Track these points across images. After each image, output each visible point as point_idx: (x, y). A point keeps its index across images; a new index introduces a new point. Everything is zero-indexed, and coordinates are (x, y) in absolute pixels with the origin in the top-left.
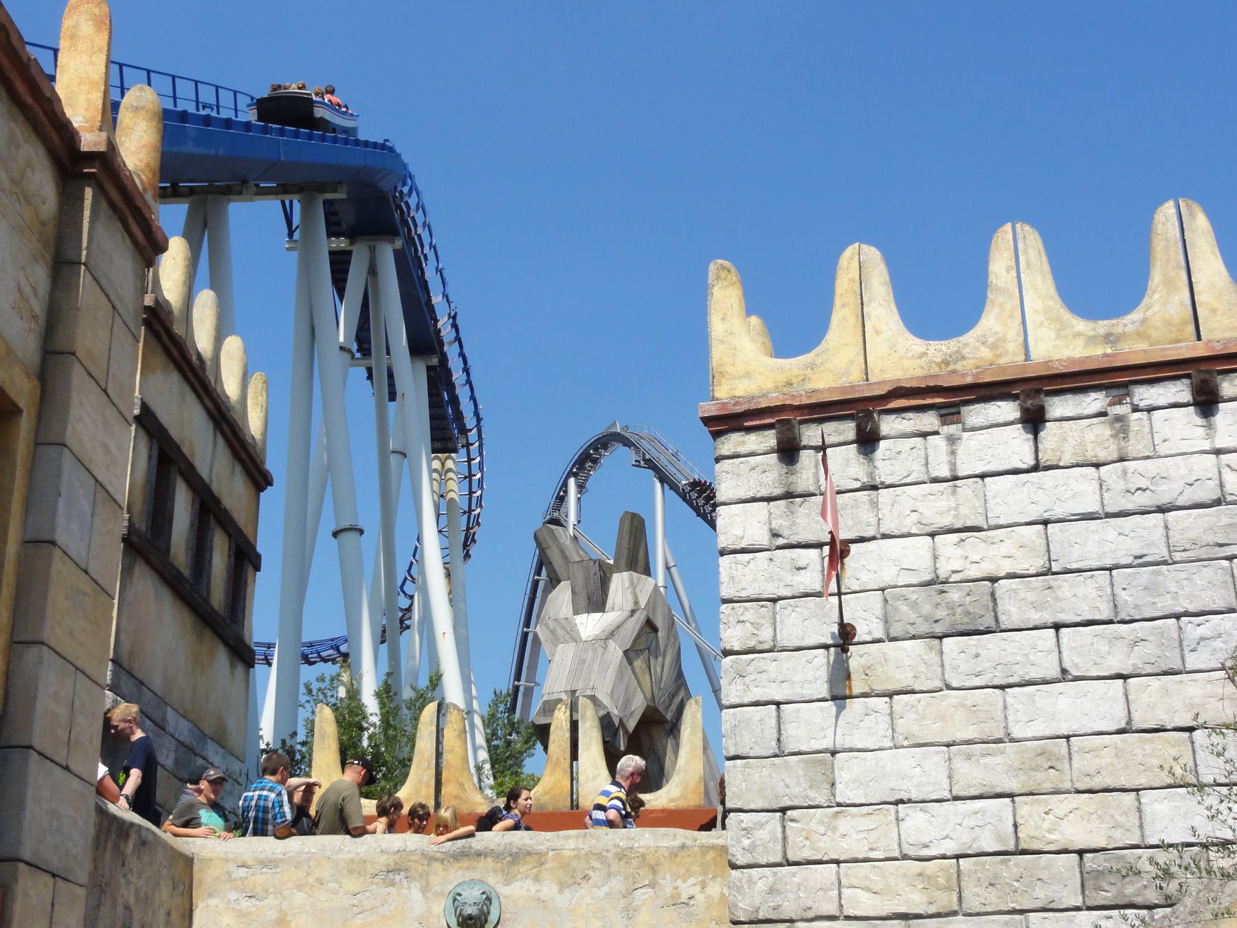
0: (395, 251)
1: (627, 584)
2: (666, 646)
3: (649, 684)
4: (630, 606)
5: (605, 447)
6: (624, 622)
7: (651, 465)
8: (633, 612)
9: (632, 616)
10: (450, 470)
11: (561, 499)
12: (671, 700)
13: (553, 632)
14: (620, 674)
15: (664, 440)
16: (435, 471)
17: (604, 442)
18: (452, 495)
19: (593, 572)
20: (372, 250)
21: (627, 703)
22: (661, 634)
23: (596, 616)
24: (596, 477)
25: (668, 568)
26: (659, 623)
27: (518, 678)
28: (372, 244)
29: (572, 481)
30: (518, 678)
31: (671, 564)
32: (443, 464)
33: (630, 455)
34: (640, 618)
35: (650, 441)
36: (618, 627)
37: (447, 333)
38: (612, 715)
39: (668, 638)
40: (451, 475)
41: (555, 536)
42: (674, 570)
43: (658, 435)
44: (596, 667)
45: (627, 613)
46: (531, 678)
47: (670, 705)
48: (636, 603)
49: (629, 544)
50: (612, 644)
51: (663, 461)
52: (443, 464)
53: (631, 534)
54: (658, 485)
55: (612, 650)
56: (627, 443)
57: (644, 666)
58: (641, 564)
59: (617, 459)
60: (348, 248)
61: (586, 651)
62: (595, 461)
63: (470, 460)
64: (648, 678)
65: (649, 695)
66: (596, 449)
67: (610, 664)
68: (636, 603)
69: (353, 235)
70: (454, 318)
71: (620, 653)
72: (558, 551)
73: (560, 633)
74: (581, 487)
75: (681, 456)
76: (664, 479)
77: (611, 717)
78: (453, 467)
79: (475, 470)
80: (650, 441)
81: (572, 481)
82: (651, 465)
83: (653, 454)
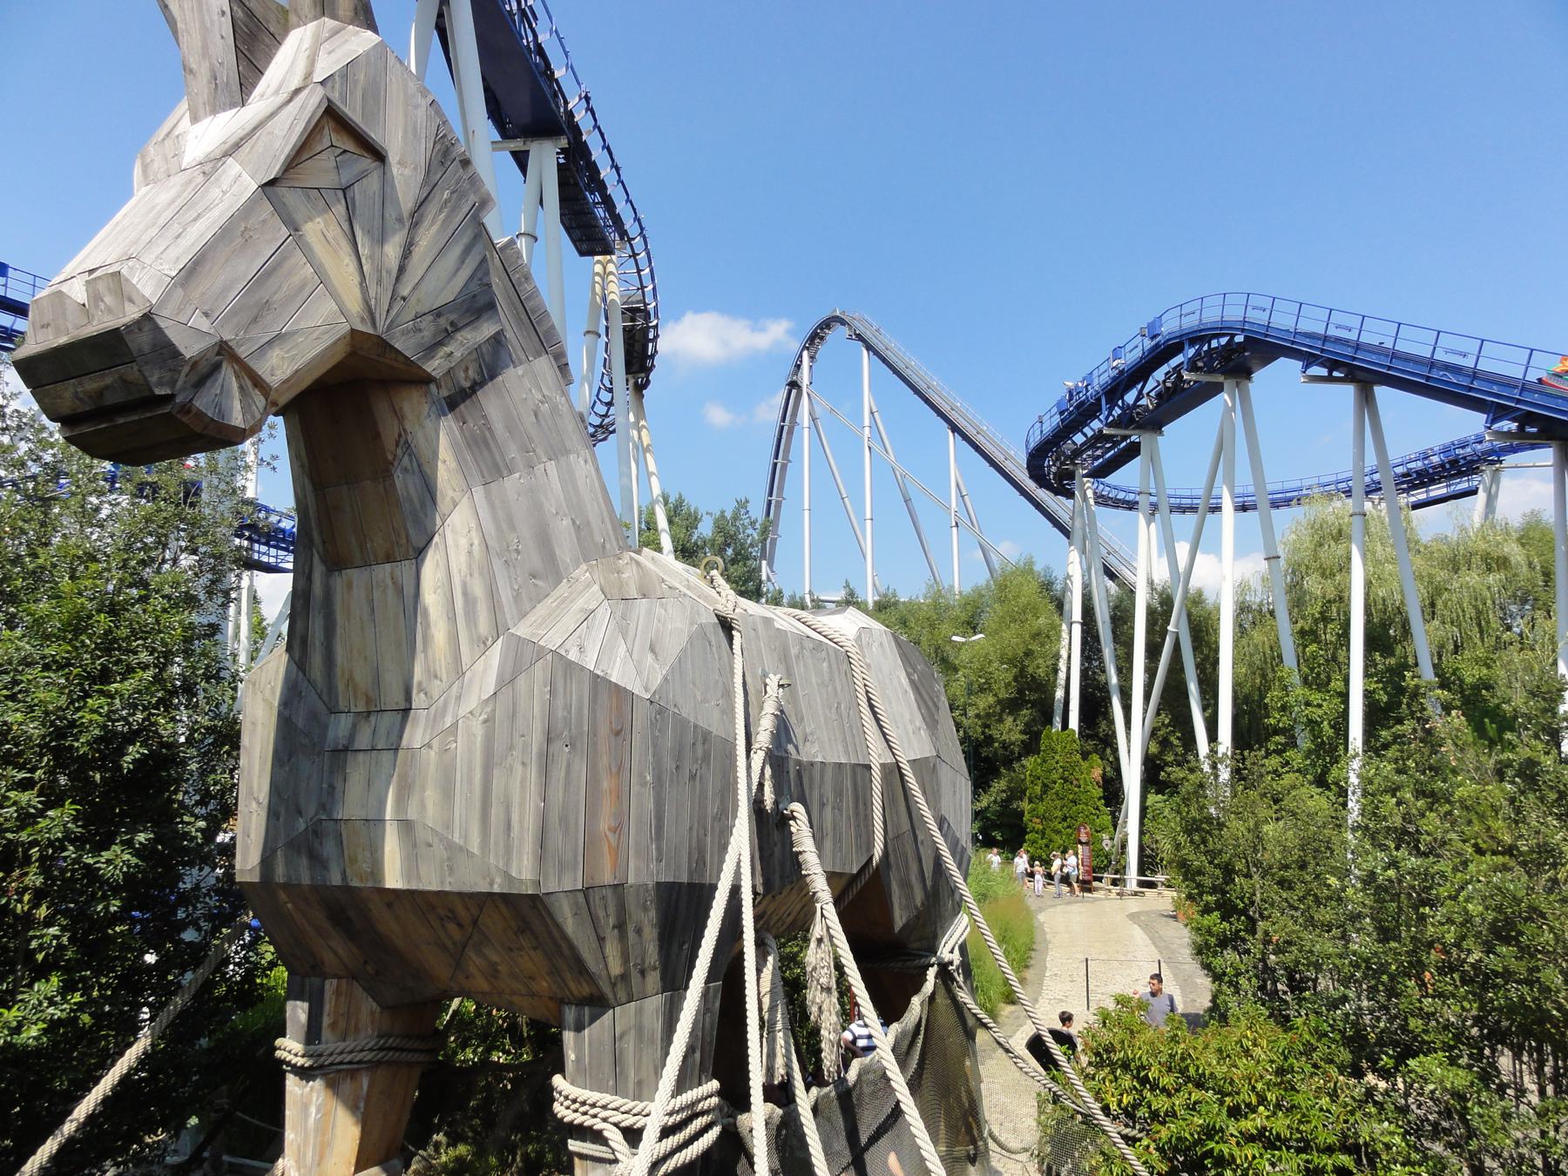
2: (421, 204)
4: (295, 83)
5: (828, 327)
7: (860, 337)
10: (611, 273)
11: (798, 367)
12: (446, 336)
14: (232, 233)
16: (598, 274)
17: (827, 324)
18: (612, 296)
19: (216, 10)
21: (256, 307)
24: (823, 349)
25: (872, 413)
27: (771, 494)
29: (805, 353)
30: (771, 494)
32: (605, 268)
33: (845, 331)
34: (310, 103)
35: (859, 321)
36: (255, 129)
37: (581, 116)
38: (162, 324)
40: (611, 278)
46: (780, 494)
47: (440, 344)
51: (868, 335)
52: (605, 268)
54: (865, 352)
55: (226, 182)
56: (843, 322)
59: (838, 334)
62: (822, 338)
63: (639, 271)
65: (354, 305)
66: (822, 329)
67: (208, 209)
68: (308, 75)
70: (587, 99)
74: (812, 358)
76: (869, 348)
77: (158, 329)
78: (614, 270)
79: (647, 281)
80: (859, 321)
81: (805, 353)
82: (860, 337)
83: (861, 330)
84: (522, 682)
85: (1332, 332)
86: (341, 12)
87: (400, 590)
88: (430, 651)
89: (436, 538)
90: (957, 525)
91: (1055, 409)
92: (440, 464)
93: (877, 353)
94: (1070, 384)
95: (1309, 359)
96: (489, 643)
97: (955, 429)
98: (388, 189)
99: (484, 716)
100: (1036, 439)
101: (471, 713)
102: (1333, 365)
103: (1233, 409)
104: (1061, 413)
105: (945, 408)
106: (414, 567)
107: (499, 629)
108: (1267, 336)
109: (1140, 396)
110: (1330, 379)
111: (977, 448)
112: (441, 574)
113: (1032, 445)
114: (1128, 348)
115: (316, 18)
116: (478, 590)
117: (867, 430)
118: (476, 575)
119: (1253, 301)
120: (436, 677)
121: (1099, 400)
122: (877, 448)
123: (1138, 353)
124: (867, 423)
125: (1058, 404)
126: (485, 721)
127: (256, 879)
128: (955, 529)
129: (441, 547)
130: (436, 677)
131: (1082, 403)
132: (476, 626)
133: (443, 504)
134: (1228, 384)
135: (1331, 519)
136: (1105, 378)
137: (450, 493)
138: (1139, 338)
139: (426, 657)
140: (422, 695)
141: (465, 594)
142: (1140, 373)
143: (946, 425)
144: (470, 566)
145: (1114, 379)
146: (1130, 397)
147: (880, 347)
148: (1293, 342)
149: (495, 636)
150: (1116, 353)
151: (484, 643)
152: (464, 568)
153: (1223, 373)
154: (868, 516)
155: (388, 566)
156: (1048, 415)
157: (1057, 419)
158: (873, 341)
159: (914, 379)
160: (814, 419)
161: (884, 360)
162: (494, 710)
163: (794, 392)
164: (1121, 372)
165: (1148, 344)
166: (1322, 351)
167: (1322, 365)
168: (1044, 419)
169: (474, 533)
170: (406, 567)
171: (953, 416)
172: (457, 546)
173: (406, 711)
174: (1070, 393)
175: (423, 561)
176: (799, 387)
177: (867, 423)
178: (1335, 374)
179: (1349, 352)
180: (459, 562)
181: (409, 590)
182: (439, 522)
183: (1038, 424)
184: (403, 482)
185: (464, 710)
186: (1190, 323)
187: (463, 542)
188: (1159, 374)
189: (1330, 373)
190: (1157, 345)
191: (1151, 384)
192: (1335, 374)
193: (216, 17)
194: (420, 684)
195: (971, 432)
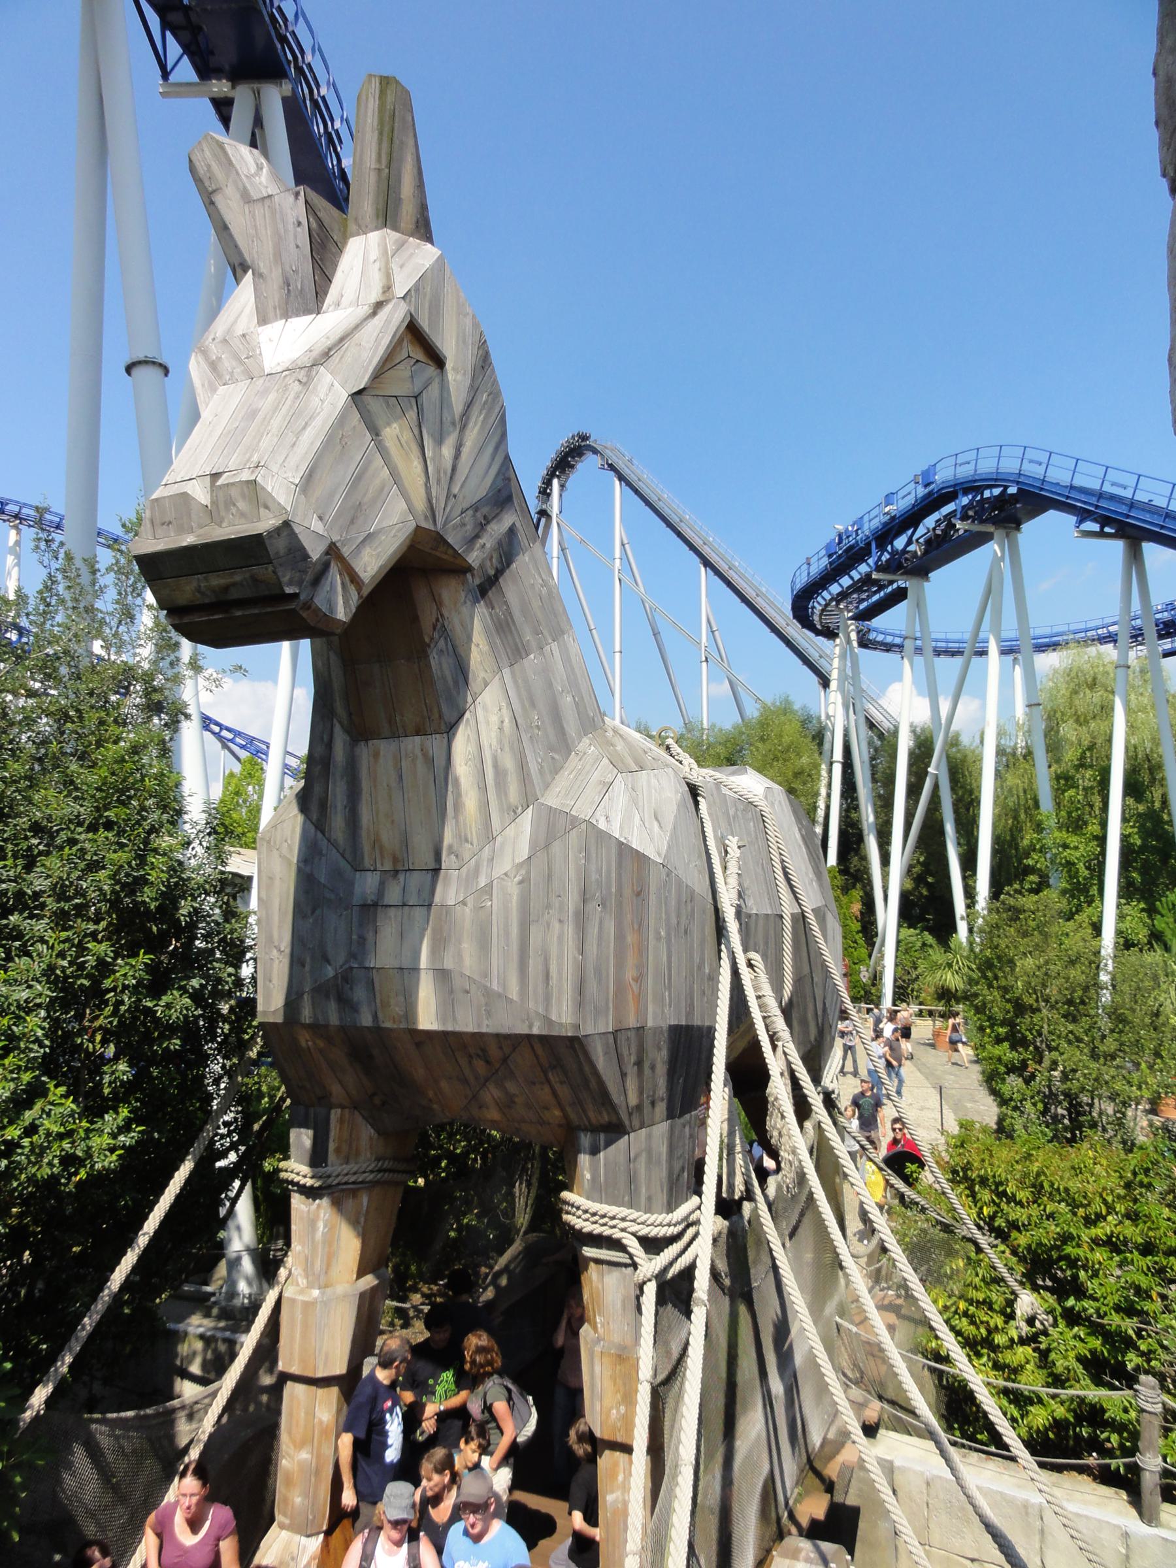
0: (285, 100)
1: (374, 253)
2: (469, 406)
3: (421, 480)
4: (375, 295)
6: (357, 327)
7: (612, 467)
8: (379, 305)
9: (374, 313)
12: (481, 527)
13: (214, 366)
14: (335, 441)
15: (622, 450)
19: (291, 220)
20: (257, 95)
21: (355, 512)
22: (457, 376)
23: (300, 322)
25: (623, 545)
26: (448, 345)
28: (255, 86)
31: (625, 541)
34: (393, 317)
36: (342, 339)
38: (297, 529)
39: (474, 390)
41: (230, 163)
42: (627, 546)
43: (618, 446)
44: (276, 423)
45: (366, 310)
47: (477, 536)
48: (388, 288)
49: (379, 160)
50: (325, 376)
51: (620, 465)
53: (381, 134)
54: (617, 482)
55: (322, 390)
57: (407, 436)
58: (408, 211)
59: (587, 466)
60: (230, 95)
61: (265, 392)
64: (417, 465)
65: (420, 505)
67: (312, 418)
68: (388, 288)
69: (237, 76)
71: (342, 396)
72: (238, 196)
73: (227, 363)
74: (562, 486)
75: (635, 462)
76: (621, 478)
77: (293, 535)
80: (612, 450)
81: (555, 482)
82: (612, 467)
84: (556, 847)
85: (1107, 488)
86: (403, 225)
87: (429, 761)
88: (461, 818)
89: (467, 715)
90: (707, 660)
91: (823, 552)
92: (473, 647)
93: (629, 484)
94: (840, 527)
95: (1083, 515)
96: (519, 811)
97: (707, 563)
98: (445, 395)
99: (518, 878)
100: (802, 580)
101: (506, 874)
102: (1105, 521)
103: (1002, 558)
104: (830, 556)
105: (697, 542)
106: (445, 740)
107: (529, 798)
108: (1042, 489)
109: (909, 542)
110: (1101, 534)
111: (729, 584)
112: (472, 748)
113: (798, 586)
114: (901, 494)
115: (377, 228)
116: (509, 763)
117: (618, 562)
118: (507, 749)
119: (1030, 454)
120: (467, 841)
121: (869, 545)
122: (627, 579)
123: (911, 500)
124: (617, 554)
125: (827, 547)
126: (521, 882)
127: (279, 1019)
128: (704, 664)
129: (473, 723)
130: (467, 841)
131: (851, 547)
132: (506, 795)
133: (475, 683)
134: (998, 534)
135: (1086, 667)
136: (876, 523)
137: (482, 674)
138: (912, 485)
139: (457, 822)
140: (453, 857)
141: (496, 766)
142: (912, 519)
143: (698, 560)
144: (500, 742)
145: (885, 524)
146: (900, 543)
147: (632, 478)
148: (1068, 497)
149: (525, 805)
150: (889, 499)
151: (515, 812)
152: (494, 743)
153: (994, 524)
154: (617, 648)
155: (417, 739)
156: (816, 558)
157: (825, 561)
158: (626, 471)
159: (666, 511)
160: (563, 549)
161: (636, 492)
162: (529, 872)
163: (543, 520)
164: (893, 518)
165: (921, 491)
166: (1097, 507)
167: (1095, 521)
168: (812, 561)
169: (504, 710)
170: (435, 743)
171: (706, 551)
172: (488, 723)
173: (436, 871)
174: (840, 536)
175: (454, 735)
176: (549, 517)
177: (617, 554)
178: (1107, 530)
179: (1124, 509)
180: (489, 738)
181: (440, 762)
182: (469, 699)
183: (805, 566)
184: (439, 663)
185: (498, 872)
186: (965, 472)
187: (494, 719)
188: (930, 521)
189: (1102, 528)
190: (930, 493)
191: (921, 530)
192: (1107, 530)
193: (291, 227)
194: (450, 847)
195: (723, 567)
